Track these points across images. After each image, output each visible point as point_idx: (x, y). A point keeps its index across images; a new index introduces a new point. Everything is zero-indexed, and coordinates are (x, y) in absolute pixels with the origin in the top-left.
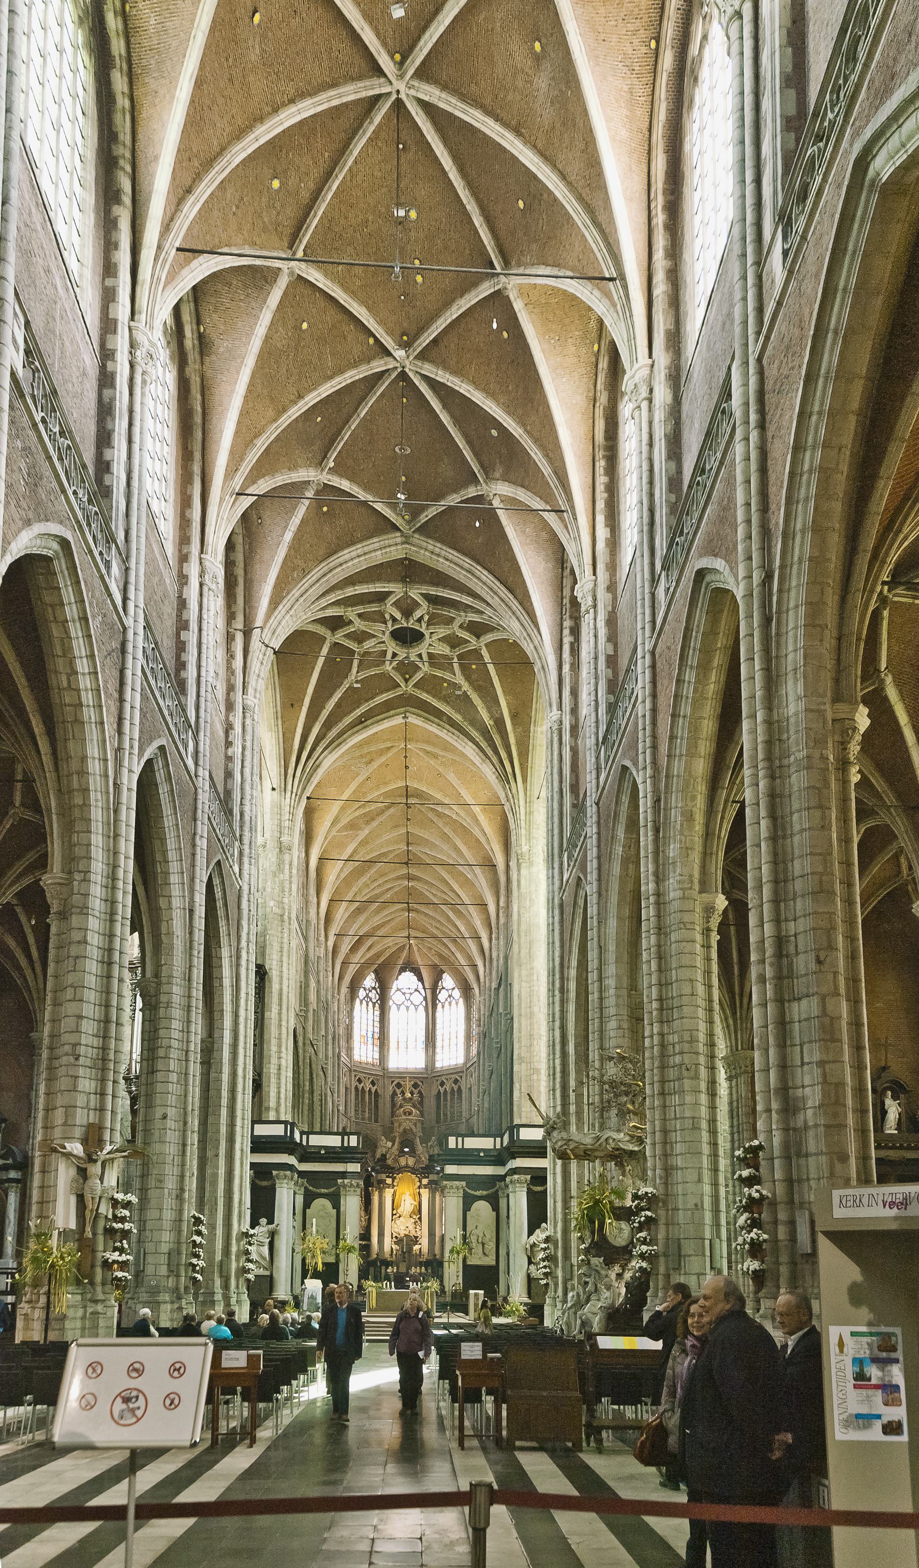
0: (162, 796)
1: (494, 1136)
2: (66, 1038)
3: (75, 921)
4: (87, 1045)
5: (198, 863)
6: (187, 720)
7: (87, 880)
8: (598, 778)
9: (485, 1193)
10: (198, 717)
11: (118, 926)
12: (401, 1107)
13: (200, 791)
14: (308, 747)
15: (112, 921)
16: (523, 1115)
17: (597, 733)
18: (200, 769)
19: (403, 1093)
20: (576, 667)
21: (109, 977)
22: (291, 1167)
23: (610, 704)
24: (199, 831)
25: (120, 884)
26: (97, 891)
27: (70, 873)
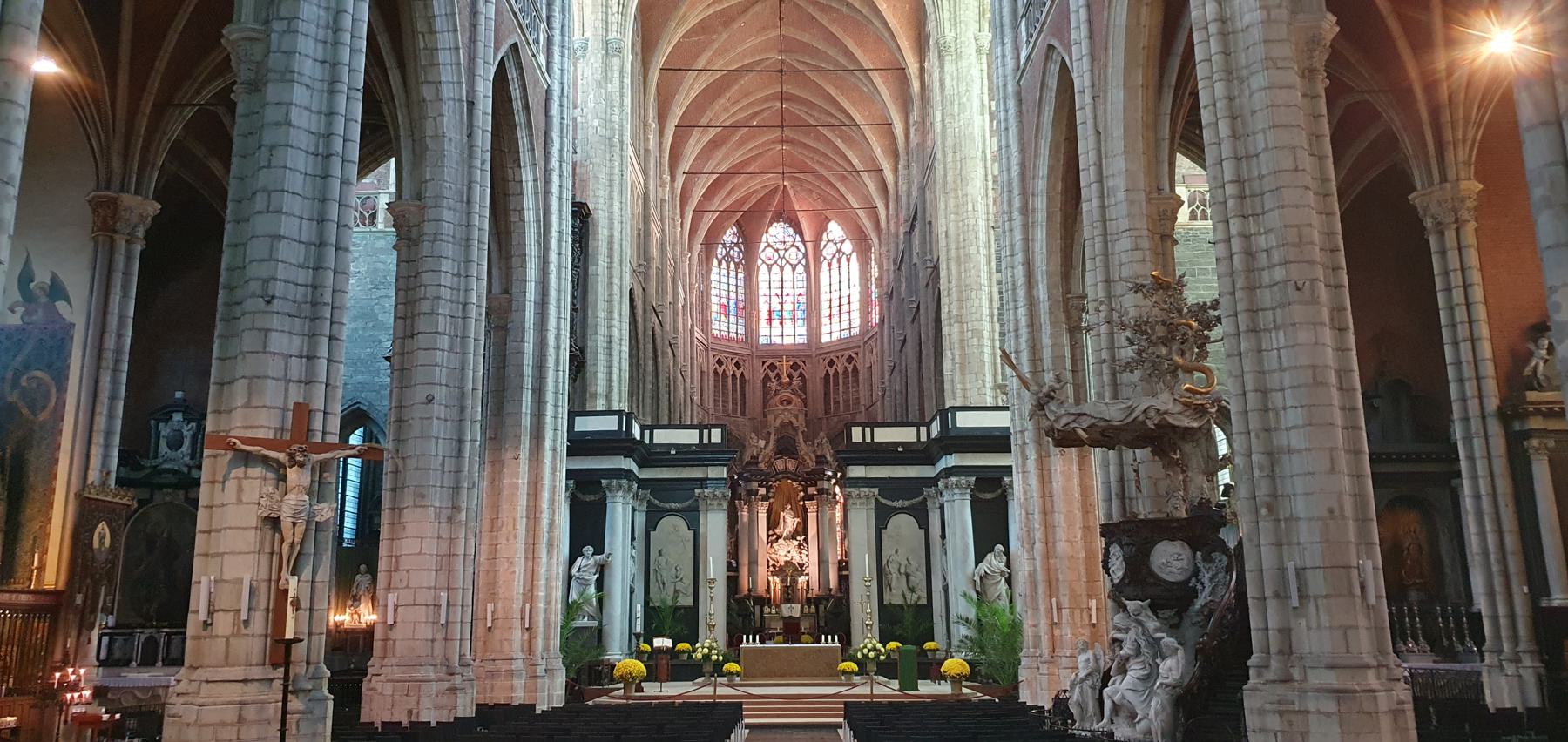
2: (255, 270)
3: (272, 92)
5: (481, 36)
11: (342, 101)
12: (776, 394)
19: (778, 377)
25: (347, 38)
27: (267, 22)
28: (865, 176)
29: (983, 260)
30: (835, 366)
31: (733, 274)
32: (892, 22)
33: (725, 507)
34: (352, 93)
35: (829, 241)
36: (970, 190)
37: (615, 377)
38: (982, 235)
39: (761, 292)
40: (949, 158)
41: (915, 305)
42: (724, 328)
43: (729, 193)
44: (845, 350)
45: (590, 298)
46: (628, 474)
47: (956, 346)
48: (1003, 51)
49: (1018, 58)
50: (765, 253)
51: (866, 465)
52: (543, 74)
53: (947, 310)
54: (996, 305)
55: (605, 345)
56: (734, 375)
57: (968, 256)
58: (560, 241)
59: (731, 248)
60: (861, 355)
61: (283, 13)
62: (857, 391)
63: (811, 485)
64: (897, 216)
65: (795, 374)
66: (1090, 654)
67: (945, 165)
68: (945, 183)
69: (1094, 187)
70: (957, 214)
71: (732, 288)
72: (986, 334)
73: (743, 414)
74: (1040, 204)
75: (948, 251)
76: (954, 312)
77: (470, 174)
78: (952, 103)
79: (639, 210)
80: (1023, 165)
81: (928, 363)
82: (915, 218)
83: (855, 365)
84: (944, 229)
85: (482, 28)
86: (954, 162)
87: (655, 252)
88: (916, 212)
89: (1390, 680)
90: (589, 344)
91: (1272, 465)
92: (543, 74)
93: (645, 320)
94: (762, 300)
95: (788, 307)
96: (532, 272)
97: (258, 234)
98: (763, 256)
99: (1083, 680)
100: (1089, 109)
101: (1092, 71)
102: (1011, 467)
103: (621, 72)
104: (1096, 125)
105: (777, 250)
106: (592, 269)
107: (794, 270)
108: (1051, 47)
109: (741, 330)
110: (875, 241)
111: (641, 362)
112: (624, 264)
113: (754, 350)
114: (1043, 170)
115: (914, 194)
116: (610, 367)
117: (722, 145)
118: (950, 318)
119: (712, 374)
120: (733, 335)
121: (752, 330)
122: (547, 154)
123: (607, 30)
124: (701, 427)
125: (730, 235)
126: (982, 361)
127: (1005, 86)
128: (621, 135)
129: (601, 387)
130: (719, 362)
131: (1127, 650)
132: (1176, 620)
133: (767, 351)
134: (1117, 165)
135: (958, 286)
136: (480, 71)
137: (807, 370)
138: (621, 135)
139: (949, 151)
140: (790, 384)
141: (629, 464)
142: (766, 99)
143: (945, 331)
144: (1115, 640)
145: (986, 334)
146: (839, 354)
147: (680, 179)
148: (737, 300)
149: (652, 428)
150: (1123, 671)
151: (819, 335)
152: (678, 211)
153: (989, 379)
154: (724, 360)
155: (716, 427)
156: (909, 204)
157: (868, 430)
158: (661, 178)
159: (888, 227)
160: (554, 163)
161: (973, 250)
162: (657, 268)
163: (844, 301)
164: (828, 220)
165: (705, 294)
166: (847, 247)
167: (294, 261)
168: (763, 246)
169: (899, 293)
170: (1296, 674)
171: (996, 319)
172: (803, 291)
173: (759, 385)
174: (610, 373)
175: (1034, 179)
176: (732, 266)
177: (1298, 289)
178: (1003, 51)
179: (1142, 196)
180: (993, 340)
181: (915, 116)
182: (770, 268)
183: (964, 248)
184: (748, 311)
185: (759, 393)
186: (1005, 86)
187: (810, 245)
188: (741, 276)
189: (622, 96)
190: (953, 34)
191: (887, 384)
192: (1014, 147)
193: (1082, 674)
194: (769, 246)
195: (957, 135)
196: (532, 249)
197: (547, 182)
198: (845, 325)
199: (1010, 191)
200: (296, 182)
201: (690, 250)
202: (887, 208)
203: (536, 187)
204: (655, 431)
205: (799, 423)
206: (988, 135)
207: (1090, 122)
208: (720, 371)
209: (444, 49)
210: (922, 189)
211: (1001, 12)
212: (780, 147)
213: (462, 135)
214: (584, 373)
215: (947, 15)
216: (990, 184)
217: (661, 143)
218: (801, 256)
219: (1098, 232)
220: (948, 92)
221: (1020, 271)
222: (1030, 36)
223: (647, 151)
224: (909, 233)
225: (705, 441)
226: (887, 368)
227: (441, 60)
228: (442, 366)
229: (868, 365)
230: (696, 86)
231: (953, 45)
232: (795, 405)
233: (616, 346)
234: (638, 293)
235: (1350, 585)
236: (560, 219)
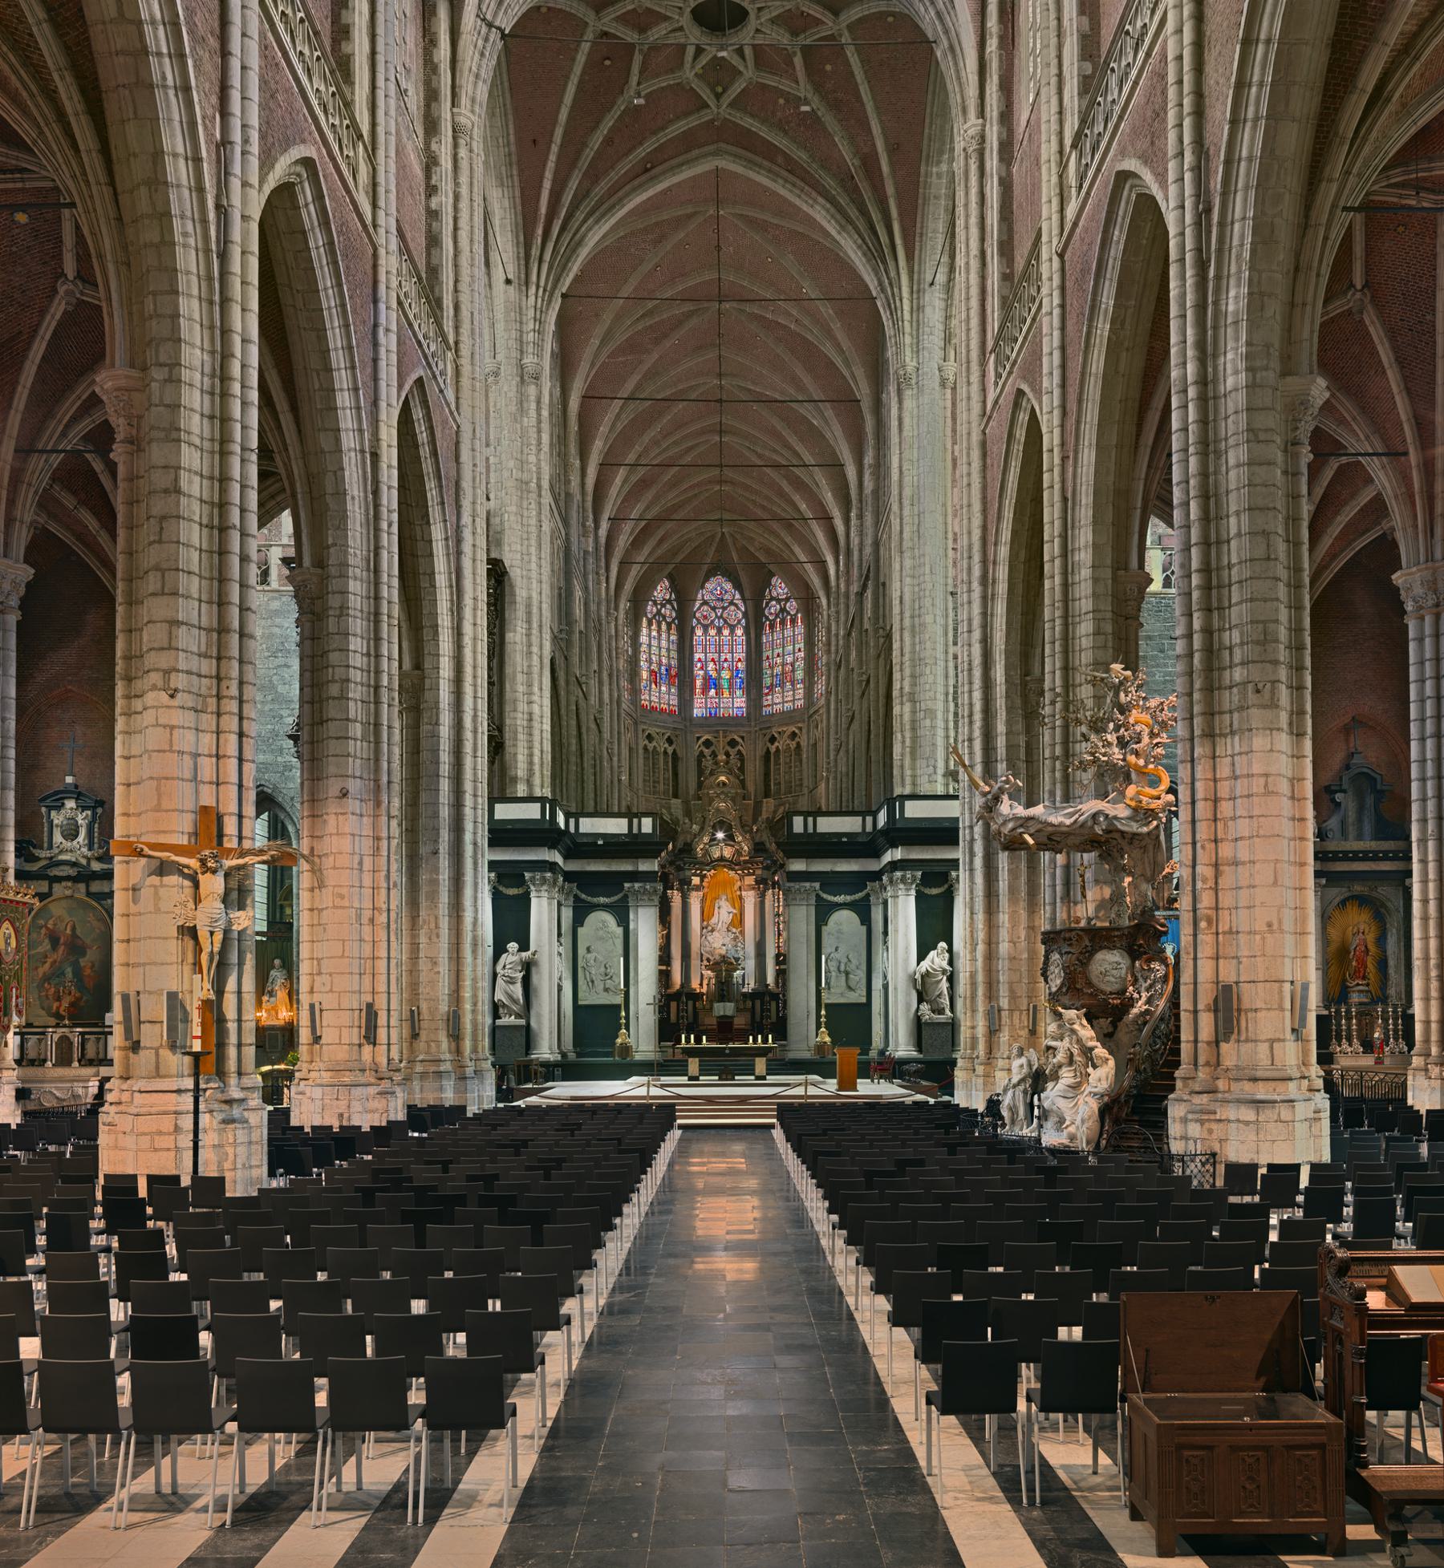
0: (314, 254)
1: (863, 814)
3: (157, 453)
4: (189, 672)
6: (354, 125)
7: (174, 381)
8: (1062, 210)
9: (849, 898)
10: (374, 125)
13: (382, 252)
14: (567, 198)
15: (224, 454)
16: (908, 780)
17: (1061, 133)
18: (381, 214)
20: (1009, 41)
21: (223, 552)
22: (552, 866)
23: (1085, 77)
24: (382, 320)
26: (194, 400)
29: (940, 631)
31: (664, 636)
32: (846, 344)
33: (657, 903)
34: (247, 454)
35: (772, 599)
40: (906, 512)
41: (865, 677)
45: (508, 670)
48: (969, 392)
49: (984, 402)
50: (700, 610)
52: (451, 413)
57: (923, 625)
58: (475, 609)
59: (663, 606)
61: (163, 358)
62: (801, 771)
63: (749, 874)
64: (848, 572)
66: (1023, 1060)
68: (901, 539)
69: (1057, 562)
70: (913, 577)
71: (664, 652)
74: (1002, 573)
77: (377, 538)
78: (911, 447)
79: (559, 563)
80: (984, 528)
81: (877, 741)
82: (867, 578)
85: (383, 364)
87: (578, 612)
89: (1310, 1090)
91: (1216, 878)
92: (451, 413)
93: (568, 692)
96: (446, 645)
97: (154, 618)
99: (1014, 1086)
100: (1057, 471)
101: (1062, 426)
102: (957, 860)
103: (539, 402)
104: (1063, 489)
105: (714, 609)
106: (509, 636)
107: (732, 632)
108: (1020, 393)
110: (824, 601)
114: (1006, 535)
115: (868, 550)
122: (458, 507)
123: (522, 352)
125: (661, 591)
127: (969, 434)
128: (539, 479)
131: (1060, 1057)
132: (1111, 1030)
134: (1084, 536)
135: (912, 660)
136: (383, 416)
138: (539, 479)
139: (906, 502)
142: (703, 432)
144: (1049, 1048)
150: (1055, 1077)
152: (603, 564)
153: (941, 765)
156: (861, 560)
158: (584, 525)
159: (838, 586)
160: (466, 519)
161: (929, 619)
162: (581, 632)
163: (788, 668)
166: (792, 606)
167: (195, 649)
169: (848, 661)
170: (1221, 1084)
175: (996, 544)
176: (664, 627)
177: (1258, 691)
178: (969, 392)
179: (1109, 572)
180: (947, 721)
181: (869, 459)
182: (706, 628)
184: (682, 675)
186: (969, 434)
188: (673, 638)
189: (539, 431)
190: (915, 364)
192: (977, 506)
193: (1015, 1080)
194: (705, 603)
196: (445, 621)
197: (459, 541)
199: (970, 558)
200: (192, 559)
201: (616, 608)
202: (837, 562)
203: (447, 546)
207: (1057, 487)
208: (650, 746)
209: (342, 390)
210: (876, 544)
211: (968, 346)
212: (717, 488)
213: (365, 491)
214: (503, 755)
215: (908, 340)
217: (583, 484)
218: (740, 615)
219: (1058, 613)
220: (905, 434)
221: (977, 650)
222: (998, 376)
223: (568, 495)
224: (861, 594)
227: (339, 404)
228: (355, 757)
230: (624, 416)
231: (914, 376)
234: (560, 661)
235: (1281, 999)
236: (474, 583)
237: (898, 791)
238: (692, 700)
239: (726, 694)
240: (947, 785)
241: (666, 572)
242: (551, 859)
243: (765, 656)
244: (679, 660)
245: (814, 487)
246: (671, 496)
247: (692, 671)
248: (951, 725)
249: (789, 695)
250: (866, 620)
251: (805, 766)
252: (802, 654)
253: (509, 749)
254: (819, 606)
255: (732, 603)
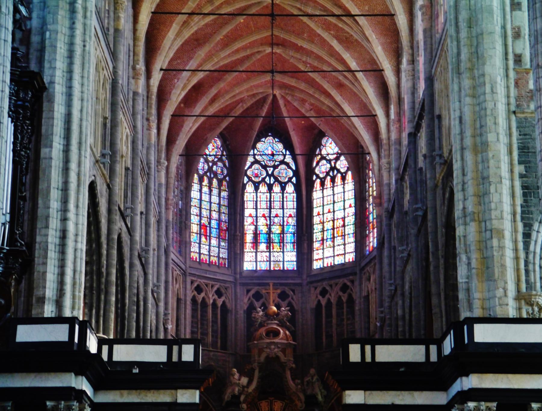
12: (261, 325)
19: (265, 307)
28: (360, 75)
29: (503, 150)
30: (327, 296)
31: (215, 192)
35: (323, 158)
36: (488, 69)
37: (68, 279)
38: (502, 120)
39: (247, 212)
40: (463, 34)
41: (420, 213)
42: (204, 251)
43: (213, 101)
44: (339, 277)
46: (80, 395)
47: (473, 248)
51: (365, 389)
53: (461, 207)
54: (519, 201)
55: (57, 241)
56: (214, 304)
59: (214, 163)
60: (357, 283)
64: (399, 120)
65: (284, 304)
67: (458, 42)
68: (459, 62)
70: (474, 96)
71: (215, 207)
72: (507, 234)
73: (224, 347)
75: (462, 140)
76: (470, 208)
82: (421, 117)
83: (350, 296)
84: (458, 114)
86: (470, 38)
88: (422, 108)
90: (38, 239)
93: (110, 222)
94: (248, 221)
95: (276, 229)
98: (249, 173)
105: (265, 167)
107: (283, 189)
109: (224, 254)
110: (374, 155)
111: (104, 270)
112: (83, 148)
113: (238, 276)
115: (422, 86)
116: (62, 266)
117: (205, 43)
118: (465, 216)
119: (189, 302)
120: (214, 259)
121: (235, 254)
124: (169, 343)
126: (503, 266)
129: (50, 292)
130: (199, 289)
133: (252, 278)
137: (296, 299)
139: (463, 25)
140: (277, 314)
141: (83, 384)
143: (459, 231)
145: (507, 234)
146: (332, 282)
147: (157, 77)
148: (219, 221)
149: (111, 343)
151: (310, 260)
152: (154, 111)
154: (204, 287)
155: (187, 342)
156: (414, 102)
157: (368, 348)
158: (134, 68)
159: (389, 138)
161: (491, 137)
163: (339, 223)
164: (322, 135)
165: (184, 213)
166: (342, 164)
168: (250, 159)
169: (402, 206)
171: (518, 217)
172: (293, 212)
173: (241, 314)
174: (62, 274)
176: (215, 182)
180: (515, 242)
183: (481, 135)
185: (242, 325)
187: (300, 159)
188: (224, 194)
191: (387, 311)
194: (256, 162)
195: (473, 8)
198: (339, 250)
201: (168, 159)
202: (387, 115)
204: (116, 347)
205: (287, 359)
206: (508, 9)
208: (200, 298)
210: (430, 80)
212: (269, 50)
214: (31, 274)
216: (511, 63)
217: (135, 30)
218: (291, 174)
225: (175, 359)
226: (386, 293)
229: (364, 293)
232: (282, 339)
233: (70, 243)
237: (464, 314)
238: (242, 253)
239: (277, 247)
240: (520, 309)
241: (219, 130)
242: (78, 387)
243: (315, 213)
244: (229, 214)
245: (365, 43)
246: (223, 54)
247: (243, 226)
248: (521, 246)
249: (339, 250)
250: (421, 158)
251: (357, 319)
252: (353, 210)
253: (38, 268)
254: (371, 161)
255: (282, 162)
